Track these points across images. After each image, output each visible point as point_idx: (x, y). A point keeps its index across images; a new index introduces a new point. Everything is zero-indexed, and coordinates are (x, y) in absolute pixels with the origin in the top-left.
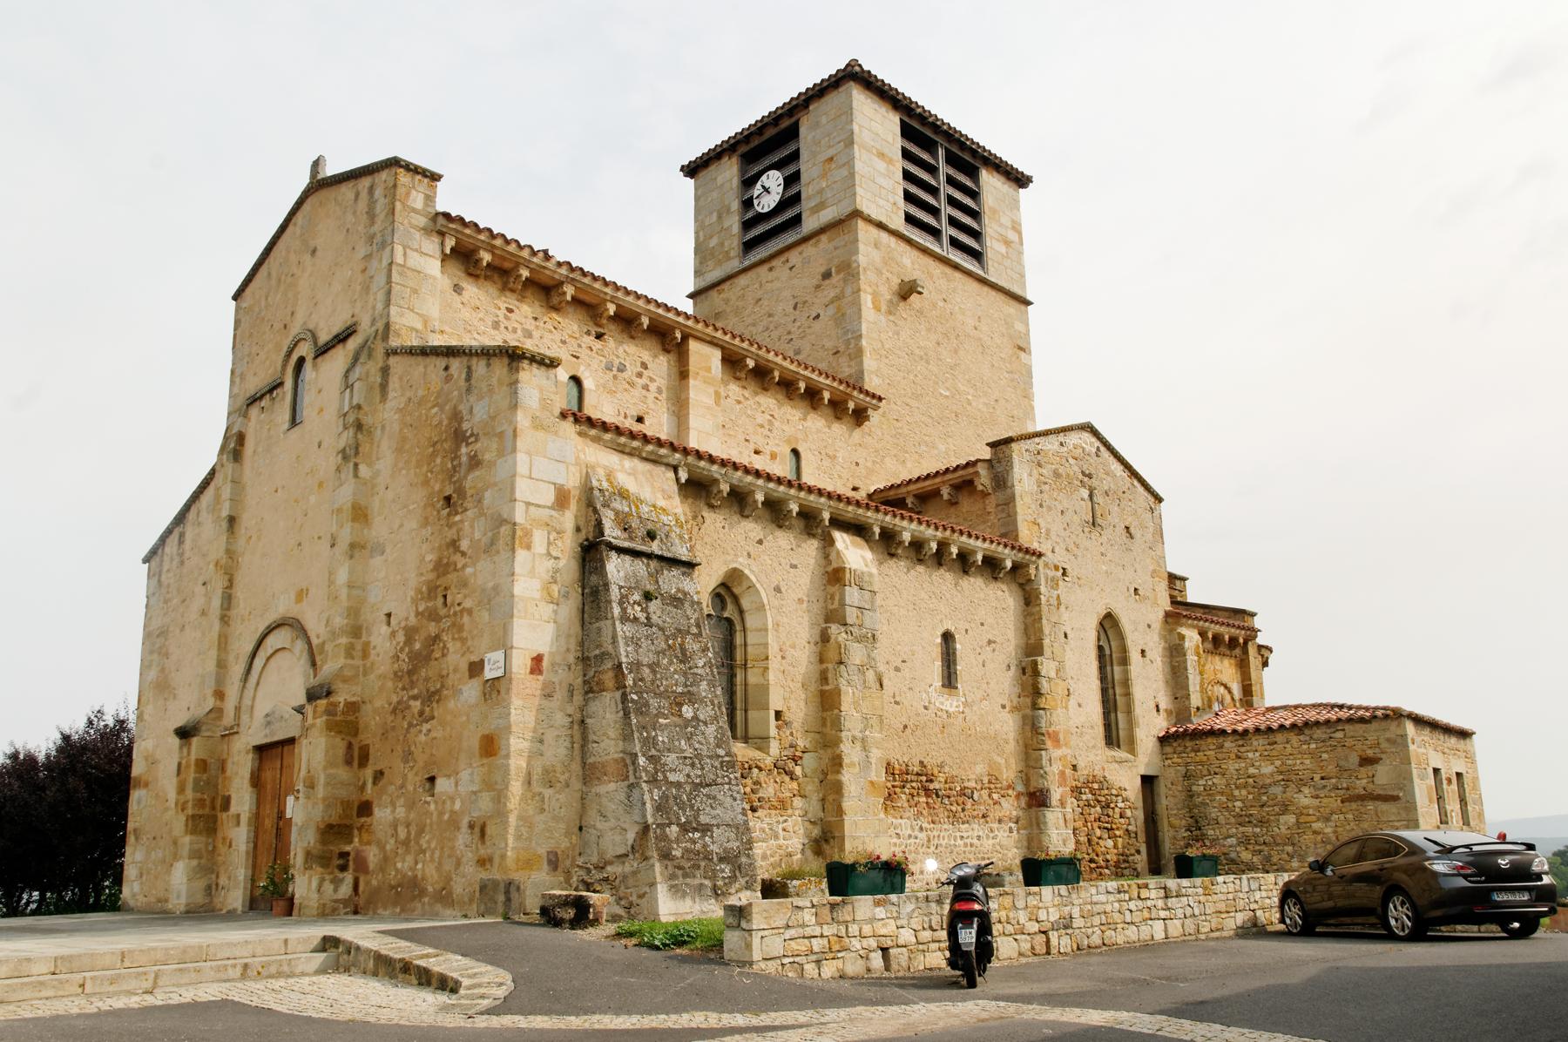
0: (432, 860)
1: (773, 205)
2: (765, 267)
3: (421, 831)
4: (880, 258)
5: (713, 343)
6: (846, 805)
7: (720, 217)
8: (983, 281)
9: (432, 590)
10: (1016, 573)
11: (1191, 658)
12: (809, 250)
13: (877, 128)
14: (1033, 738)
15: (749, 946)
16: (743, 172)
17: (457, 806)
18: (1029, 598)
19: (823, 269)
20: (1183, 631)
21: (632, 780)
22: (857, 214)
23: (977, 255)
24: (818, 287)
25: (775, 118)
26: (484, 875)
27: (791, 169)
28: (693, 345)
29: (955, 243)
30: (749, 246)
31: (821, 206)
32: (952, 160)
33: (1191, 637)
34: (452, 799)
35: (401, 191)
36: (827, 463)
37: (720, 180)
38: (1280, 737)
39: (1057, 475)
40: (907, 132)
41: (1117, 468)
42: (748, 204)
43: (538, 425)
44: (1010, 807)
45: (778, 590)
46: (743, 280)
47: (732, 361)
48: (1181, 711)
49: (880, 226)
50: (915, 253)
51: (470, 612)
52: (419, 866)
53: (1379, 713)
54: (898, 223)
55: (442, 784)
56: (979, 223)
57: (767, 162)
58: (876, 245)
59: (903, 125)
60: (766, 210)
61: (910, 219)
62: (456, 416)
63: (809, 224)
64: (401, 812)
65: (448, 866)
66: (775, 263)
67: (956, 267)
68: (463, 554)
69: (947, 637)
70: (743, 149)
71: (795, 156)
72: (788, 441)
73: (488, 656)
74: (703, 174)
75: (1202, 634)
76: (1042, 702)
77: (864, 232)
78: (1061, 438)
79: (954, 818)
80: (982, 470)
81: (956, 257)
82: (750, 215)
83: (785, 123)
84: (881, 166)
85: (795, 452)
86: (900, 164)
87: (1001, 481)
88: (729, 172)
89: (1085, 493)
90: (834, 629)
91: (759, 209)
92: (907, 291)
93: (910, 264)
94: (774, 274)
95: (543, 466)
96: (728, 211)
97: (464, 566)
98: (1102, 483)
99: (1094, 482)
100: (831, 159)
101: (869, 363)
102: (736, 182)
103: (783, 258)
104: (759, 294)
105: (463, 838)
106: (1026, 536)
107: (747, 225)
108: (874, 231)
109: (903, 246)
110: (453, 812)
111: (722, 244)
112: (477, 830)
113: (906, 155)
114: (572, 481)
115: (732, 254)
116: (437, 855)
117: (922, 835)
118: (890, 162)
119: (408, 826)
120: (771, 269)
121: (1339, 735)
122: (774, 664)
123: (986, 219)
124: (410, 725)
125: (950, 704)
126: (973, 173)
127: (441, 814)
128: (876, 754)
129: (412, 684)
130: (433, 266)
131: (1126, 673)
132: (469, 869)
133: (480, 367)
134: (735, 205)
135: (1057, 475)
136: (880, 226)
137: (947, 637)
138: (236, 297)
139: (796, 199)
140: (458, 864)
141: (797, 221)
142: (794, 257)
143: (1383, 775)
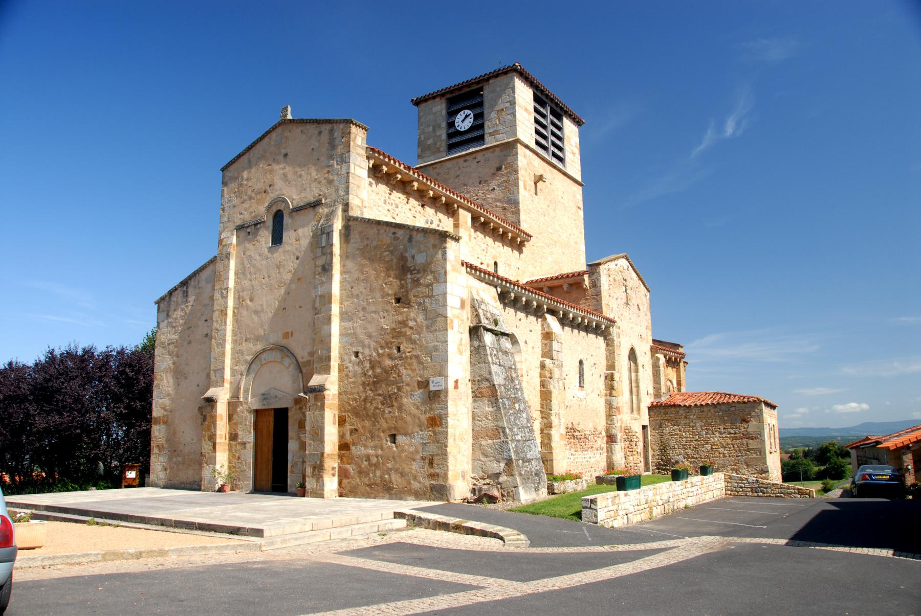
1: (467, 128)
2: (462, 160)
4: (528, 163)
5: (468, 209)
6: (553, 445)
7: (434, 129)
8: (565, 174)
10: (601, 329)
11: (662, 369)
12: (488, 154)
13: (524, 94)
14: (611, 411)
15: (596, 516)
16: (448, 109)
18: (609, 343)
19: (497, 165)
20: (658, 355)
21: (503, 439)
22: (518, 141)
23: (561, 160)
24: (494, 174)
25: (469, 84)
27: (478, 111)
28: (461, 211)
29: (554, 155)
30: (451, 147)
31: (496, 132)
32: (553, 113)
33: (662, 360)
35: (352, 136)
36: (507, 268)
37: (434, 110)
38: (705, 409)
39: (615, 280)
40: (537, 99)
41: (634, 275)
42: (451, 125)
43: (455, 270)
44: (602, 442)
45: (526, 342)
46: (448, 164)
47: (475, 219)
48: (657, 394)
49: (527, 147)
50: (539, 160)
53: (751, 399)
54: (533, 145)
55: (400, 439)
56: (563, 143)
57: (462, 105)
58: (525, 157)
59: (535, 95)
60: (463, 130)
61: (538, 143)
62: (403, 258)
63: (490, 142)
66: (467, 158)
67: (555, 167)
68: (411, 328)
69: (581, 362)
70: (449, 96)
71: (481, 104)
72: (493, 258)
74: (423, 105)
75: (665, 357)
76: (614, 393)
77: (521, 149)
78: (616, 262)
79: (583, 450)
80: (586, 277)
81: (555, 161)
82: (452, 130)
83: (475, 87)
84: (526, 115)
85: (496, 264)
86: (533, 114)
87: (595, 284)
88: (440, 107)
89: (624, 289)
90: (548, 362)
91: (459, 129)
92: (540, 178)
93: (540, 167)
95: (459, 288)
96: (439, 126)
98: (630, 284)
99: (627, 283)
101: (522, 217)
102: (444, 112)
103: (474, 156)
104: (459, 173)
106: (607, 313)
107: (450, 136)
108: (524, 148)
109: (535, 157)
111: (435, 144)
112: (427, 461)
113: (536, 110)
114: (466, 296)
115: (442, 149)
117: (572, 457)
118: (529, 113)
120: (465, 161)
121: (733, 409)
122: (525, 378)
123: (566, 142)
125: (581, 394)
126: (560, 119)
128: (563, 420)
130: (364, 173)
131: (637, 376)
134: (444, 124)
135: (615, 280)
136: (527, 147)
137: (581, 362)
138: (223, 170)
139: (481, 126)
141: (481, 139)
142: (480, 157)
143: (752, 427)
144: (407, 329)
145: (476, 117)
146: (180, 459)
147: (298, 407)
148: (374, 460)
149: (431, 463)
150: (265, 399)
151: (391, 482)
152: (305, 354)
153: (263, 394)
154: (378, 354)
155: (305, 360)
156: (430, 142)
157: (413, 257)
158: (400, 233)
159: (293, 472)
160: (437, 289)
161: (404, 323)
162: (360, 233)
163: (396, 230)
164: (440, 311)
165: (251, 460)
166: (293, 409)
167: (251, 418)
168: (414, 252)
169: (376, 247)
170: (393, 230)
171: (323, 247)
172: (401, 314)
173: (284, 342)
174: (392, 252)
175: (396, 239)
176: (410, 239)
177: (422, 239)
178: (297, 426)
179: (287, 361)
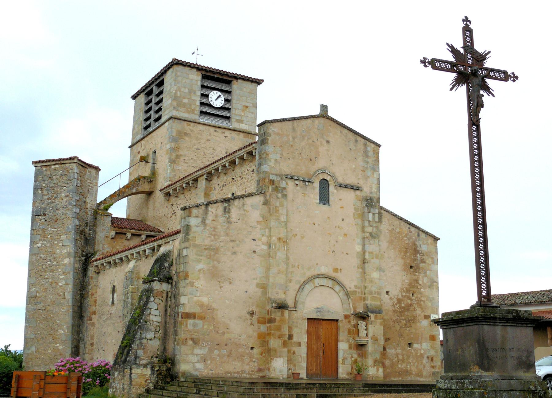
0: (414, 365)
3: (408, 357)
9: (408, 291)
17: (422, 352)
26: (433, 370)
31: (240, 121)
34: (420, 350)
51: (424, 302)
52: (409, 367)
55: (415, 346)
60: (214, 105)
62: (414, 244)
64: (399, 351)
65: (421, 367)
68: (420, 285)
73: (432, 315)
94: (215, 134)
96: (195, 93)
97: (421, 288)
100: (247, 107)
104: (209, 138)
105: (425, 361)
110: (421, 354)
112: (430, 359)
115: (196, 112)
116: (416, 364)
119: (403, 355)
120: (216, 131)
124: (401, 327)
127: (416, 354)
129: (402, 316)
132: (428, 368)
133: (423, 235)
140: (424, 367)
144: (418, 285)
145: (227, 101)
146: (225, 352)
147: (347, 320)
148: (400, 357)
149: (432, 360)
150: (319, 311)
151: (411, 370)
152: (353, 287)
153: (317, 308)
154: (402, 296)
155: (351, 290)
156: (185, 101)
157: (421, 246)
158: (413, 229)
159: (343, 364)
160: (433, 267)
161: (417, 281)
162: (388, 220)
163: (411, 227)
164: (435, 279)
165: (304, 355)
166: (344, 321)
167: (304, 325)
168: (421, 243)
169: (399, 233)
170: (408, 226)
171: (370, 221)
172: (415, 275)
173: (334, 275)
174: (409, 239)
175: (411, 232)
176: (418, 235)
177: (424, 237)
178: (347, 333)
179: (337, 288)
